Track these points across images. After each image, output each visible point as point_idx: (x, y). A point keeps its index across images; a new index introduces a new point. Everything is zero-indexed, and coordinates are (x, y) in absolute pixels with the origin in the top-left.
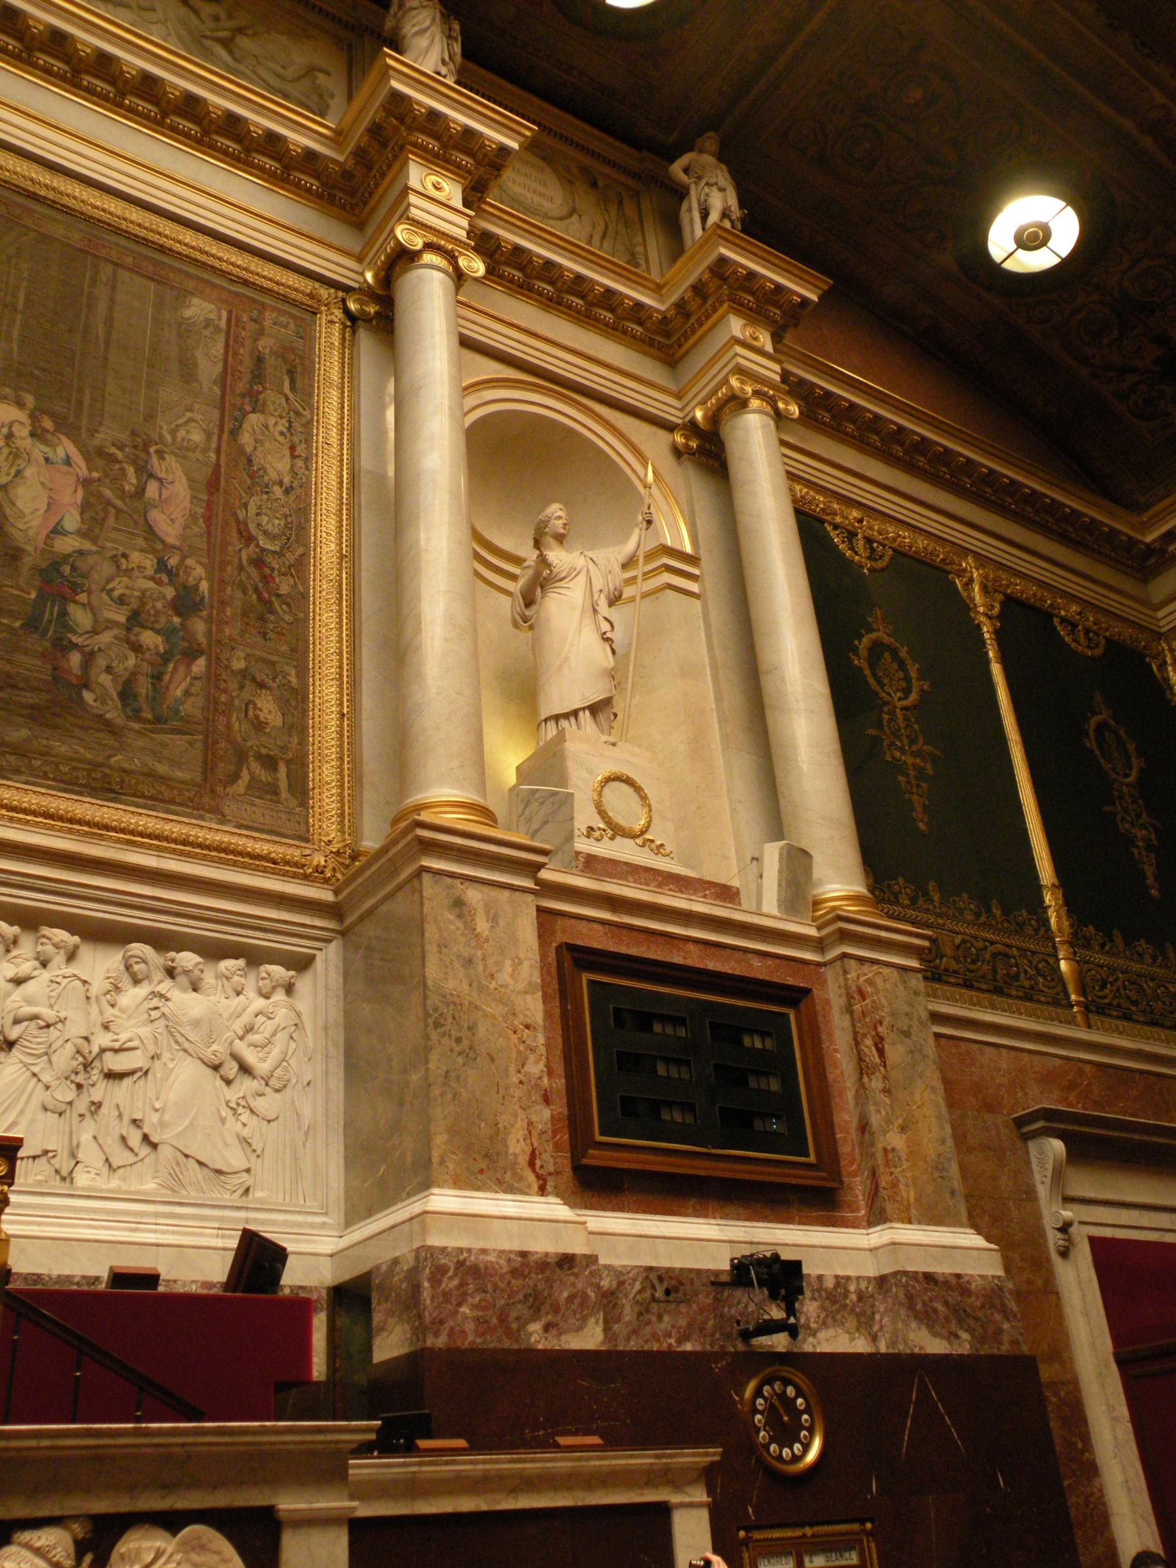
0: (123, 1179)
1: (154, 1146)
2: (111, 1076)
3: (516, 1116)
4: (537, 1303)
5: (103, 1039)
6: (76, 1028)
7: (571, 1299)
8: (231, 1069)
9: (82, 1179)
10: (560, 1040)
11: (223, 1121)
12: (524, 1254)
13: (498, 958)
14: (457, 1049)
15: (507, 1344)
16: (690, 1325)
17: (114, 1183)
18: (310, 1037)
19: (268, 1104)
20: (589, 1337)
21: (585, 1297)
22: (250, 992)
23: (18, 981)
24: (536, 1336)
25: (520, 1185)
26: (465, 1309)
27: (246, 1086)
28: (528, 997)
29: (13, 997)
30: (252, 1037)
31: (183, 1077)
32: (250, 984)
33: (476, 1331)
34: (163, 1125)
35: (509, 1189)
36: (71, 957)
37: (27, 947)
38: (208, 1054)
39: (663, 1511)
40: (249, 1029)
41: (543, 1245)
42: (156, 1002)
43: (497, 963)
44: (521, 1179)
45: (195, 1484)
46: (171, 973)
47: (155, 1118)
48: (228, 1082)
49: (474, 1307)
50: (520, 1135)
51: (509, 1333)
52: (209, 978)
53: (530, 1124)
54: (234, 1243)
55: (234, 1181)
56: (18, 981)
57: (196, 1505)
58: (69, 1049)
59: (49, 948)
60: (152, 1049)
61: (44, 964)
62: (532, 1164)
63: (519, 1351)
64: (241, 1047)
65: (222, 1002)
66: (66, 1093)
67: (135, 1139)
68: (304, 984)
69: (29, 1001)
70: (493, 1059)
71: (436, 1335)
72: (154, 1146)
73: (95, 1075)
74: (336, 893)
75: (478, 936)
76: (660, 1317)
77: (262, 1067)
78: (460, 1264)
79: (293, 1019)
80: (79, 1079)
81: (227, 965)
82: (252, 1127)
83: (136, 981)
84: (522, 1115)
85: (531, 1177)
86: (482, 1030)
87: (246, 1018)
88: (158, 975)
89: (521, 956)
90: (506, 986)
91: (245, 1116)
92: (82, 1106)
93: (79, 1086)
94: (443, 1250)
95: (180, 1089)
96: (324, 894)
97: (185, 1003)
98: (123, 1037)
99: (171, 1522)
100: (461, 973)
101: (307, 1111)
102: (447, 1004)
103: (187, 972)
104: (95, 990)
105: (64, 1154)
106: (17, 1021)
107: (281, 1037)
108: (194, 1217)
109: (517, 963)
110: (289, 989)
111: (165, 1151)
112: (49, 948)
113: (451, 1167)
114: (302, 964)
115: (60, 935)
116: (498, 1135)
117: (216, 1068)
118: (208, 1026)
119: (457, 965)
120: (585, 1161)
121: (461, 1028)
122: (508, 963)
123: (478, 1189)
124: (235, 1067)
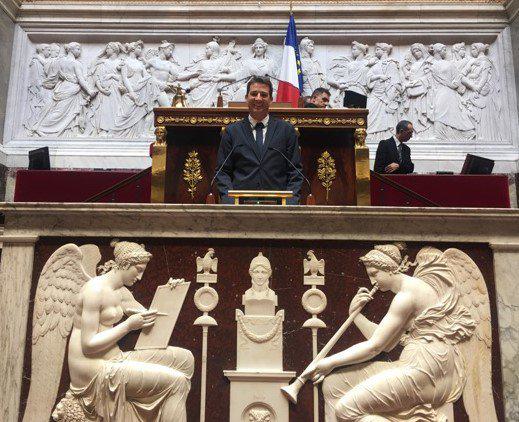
1: (433, 123)
2: (411, 97)
5: (407, 84)
6: (395, 81)
8: (463, 89)
18: (499, 71)
22: (468, 57)
23: (370, 66)
27: (471, 95)
31: (442, 95)
32: (468, 53)
34: (435, 114)
36: (390, 53)
37: (372, 52)
38: (452, 85)
40: (469, 72)
45: (450, 233)
46: (432, 53)
48: (462, 95)
52: (449, 53)
54: (465, 158)
55: (468, 133)
56: (370, 66)
57: (451, 240)
58: (393, 88)
59: (380, 51)
60: (427, 84)
65: (458, 62)
66: (396, 106)
67: (424, 120)
68: (493, 49)
69: (375, 73)
72: (433, 123)
73: (405, 98)
74: (505, 6)
79: (489, 64)
81: (456, 46)
82: (475, 112)
83: (418, 59)
87: (468, 67)
88: (427, 55)
92: (401, 110)
93: (399, 103)
95: (442, 102)
96: (501, 8)
97: (439, 64)
98: (415, 82)
99: (442, 246)
101: (499, 103)
103: (439, 52)
104: (401, 65)
106: (371, 81)
108: (452, 149)
110: (486, 52)
111: (437, 124)
112: (380, 51)
114: (491, 40)
115: (384, 45)
117: (456, 89)
118: (450, 72)
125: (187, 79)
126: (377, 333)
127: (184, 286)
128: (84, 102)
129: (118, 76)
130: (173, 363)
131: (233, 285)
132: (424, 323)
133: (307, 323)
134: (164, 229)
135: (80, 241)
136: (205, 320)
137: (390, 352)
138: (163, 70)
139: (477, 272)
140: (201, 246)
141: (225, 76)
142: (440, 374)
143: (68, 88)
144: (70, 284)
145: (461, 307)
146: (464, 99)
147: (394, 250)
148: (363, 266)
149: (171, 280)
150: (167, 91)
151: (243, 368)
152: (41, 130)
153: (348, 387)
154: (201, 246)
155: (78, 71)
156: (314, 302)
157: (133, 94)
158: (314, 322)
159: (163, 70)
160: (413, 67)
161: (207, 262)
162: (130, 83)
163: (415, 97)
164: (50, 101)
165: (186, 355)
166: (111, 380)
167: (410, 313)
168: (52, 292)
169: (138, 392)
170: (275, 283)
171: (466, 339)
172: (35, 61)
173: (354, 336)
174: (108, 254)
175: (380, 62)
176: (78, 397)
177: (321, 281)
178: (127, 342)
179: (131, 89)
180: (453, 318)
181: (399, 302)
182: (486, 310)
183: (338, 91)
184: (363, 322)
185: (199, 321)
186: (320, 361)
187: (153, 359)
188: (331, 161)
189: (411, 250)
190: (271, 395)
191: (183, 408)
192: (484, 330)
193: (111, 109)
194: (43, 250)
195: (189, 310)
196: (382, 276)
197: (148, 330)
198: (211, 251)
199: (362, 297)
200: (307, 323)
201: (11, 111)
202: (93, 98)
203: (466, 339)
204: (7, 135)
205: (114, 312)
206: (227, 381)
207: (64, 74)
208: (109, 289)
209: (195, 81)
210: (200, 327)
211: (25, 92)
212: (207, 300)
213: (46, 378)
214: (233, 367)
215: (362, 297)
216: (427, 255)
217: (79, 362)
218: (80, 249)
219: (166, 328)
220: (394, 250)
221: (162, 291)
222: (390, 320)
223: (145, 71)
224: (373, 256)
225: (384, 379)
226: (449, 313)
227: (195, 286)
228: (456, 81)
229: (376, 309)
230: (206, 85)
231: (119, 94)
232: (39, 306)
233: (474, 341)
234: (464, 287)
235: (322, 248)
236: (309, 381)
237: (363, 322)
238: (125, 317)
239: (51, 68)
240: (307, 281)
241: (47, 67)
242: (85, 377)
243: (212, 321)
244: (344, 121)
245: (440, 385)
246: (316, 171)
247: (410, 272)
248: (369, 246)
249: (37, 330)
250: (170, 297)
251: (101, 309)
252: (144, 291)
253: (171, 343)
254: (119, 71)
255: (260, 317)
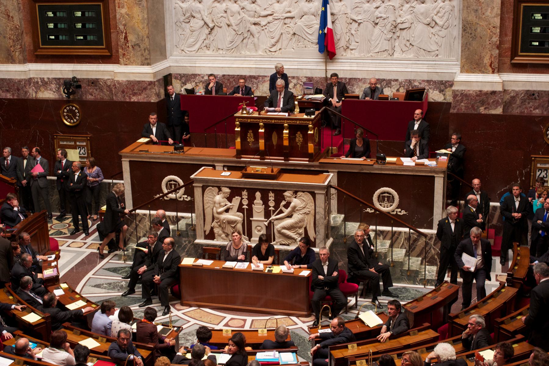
0: (406, 54)
3: (487, 53)
4: (483, 103)
5: (399, 21)
6: (392, 18)
7: (493, 102)
8: (433, 24)
9: (396, 55)
10: (512, 25)
11: (431, 38)
12: (480, 91)
13: (486, 8)
14: (470, 36)
15: (473, 112)
16: (539, 105)
17: (404, 56)
19: (443, 33)
20: (499, 111)
21: (498, 101)
23: (377, 8)
24: (482, 110)
25: (487, 71)
26: (462, 104)
27: (437, 28)
28: (495, 18)
29: (377, 12)
30: (439, 14)
31: (419, 28)
33: (465, 109)
35: (483, 72)
39: (434, 177)
40: (438, 12)
41: (487, 88)
42: (412, 9)
43: (486, 10)
44: (487, 69)
47: (413, 39)
48: (432, 27)
49: (464, 104)
50: (488, 58)
51: (474, 109)
53: (492, 55)
55: (433, 53)
56: (377, 8)
58: (390, 24)
60: (411, 21)
61: (383, 2)
62: (491, 65)
63: (475, 114)
64: (435, 18)
66: (390, 35)
67: (408, 44)
69: (380, 13)
70: (481, 38)
71: (454, 109)
75: (480, 2)
76: (529, 103)
77: (440, 23)
78: (462, 94)
80: (393, 31)
83: (407, 3)
84: (489, 52)
85: (490, 69)
86: (479, 30)
87: (437, 9)
89: (494, 6)
90: (488, 16)
91: (437, 36)
92: (395, 37)
94: (457, 91)
98: (403, 19)
99: (303, 192)
100: (473, 14)
102: (468, 24)
105: (390, 49)
106: (377, 18)
107: (447, 14)
109: (493, 8)
113: (466, 67)
116: (481, 58)
118: (425, 14)
119: (472, 12)
120: (513, 62)
121: (472, 30)
122: (489, 9)
123: (473, 73)
124: (434, 23)
125: (266, 16)
126: (286, 211)
127: (239, 198)
128: (207, 31)
129: (225, 15)
130: (238, 216)
131: (251, 199)
132: (297, 210)
133: (270, 209)
134: (233, 184)
135: (213, 186)
136: (245, 207)
137: (290, 216)
138: (251, 11)
139: (312, 198)
140: (243, 189)
141: (289, 15)
142: (300, 222)
143: (197, 23)
144: (211, 197)
145: (307, 206)
146: (433, 30)
147: (291, 192)
148: (284, 196)
149: (236, 197)
150: (255, 24)
151: (254, 219)
152: (186, 49)
153: (279, 223)
154: (243, 189)
155: (202, 12)
156: (272, 204)
157: (235, 28)
158: (272, 208)
159: (251, 11)
160: (404, 8)
161: (245, 193)
162: (233, 21)
163: (404, 29)
164: (188, 31)
165: (241, 214)
166: (224, 220)
167: (294, 207)
168: (207, 198)
169: (230, 222)
170: (262, 199)
171: (308, 214)
172: (177, 5)
173: (281, 212)
174: (220, 190)
175: (383, 5)
176: (217, 222)
177: (273, 199)
178: (227, 211)
179: (233, 25)
180: (305, 209)
181: (292, 205)
182: (313, 207)
183: (357, 24)
184: (283, 209)
185: (244, 207)
186: (273, 217)
187: (233, 215)
188: (301, 135)
189: (296, 192)
190: (261, 224)
191: (241, 226)
192: (313, 212)
193: (224, 36)
194: (204, 189)
195: (241, 204)
196: (287, 199)
197: (232, 208)
198: (246, 190)
199: (283, 203)
200: (270, 209)
201: (168, 38)
202: (212, 29)
203: (308, 214)
204: (168, 53)
205: (223, 204)
206: (251, 221)
207: (194, 14)
208: (221, 199)
209: (270, 18)
210: (244, 209)
211: (174, 26)
212: (245, 202)
213: (209, 218)
214: (252, 217)
215: (283, 203)
216: (300, 194)
217: (216, 215)
218: (213, 188)
219: (236, 208)
220: (291, 192)
221: (234, 199)
222: (289, 209)
223: (241, 11)
224: (286, 194)
225: (288, 222)
226: (304, 208)
227: (242, 199)
228: (429, 20)
229: (287, 206)
230: (276, 22)
231: (227, 26)
232: (205, 202)
233: (310, 215)
234: (309, 202)
235: (274, 191)
236: (270, 222)
237: (283, 209)
238: (226, 205)
239: (187, 11)
240: (270, 198)
241: (184, 10)
242: (218, 218)
243: (247, 207)
244: (304, 122)
245: (300, 224)
246: (295, 140)
247: (295, 197)
248: (285, 191)
249: (205, 207)
250: (236, 201)
251: (220, 203)
252: (230, 199)
253: (238, 211)
254: (226, 12)
255: (258, 207)
